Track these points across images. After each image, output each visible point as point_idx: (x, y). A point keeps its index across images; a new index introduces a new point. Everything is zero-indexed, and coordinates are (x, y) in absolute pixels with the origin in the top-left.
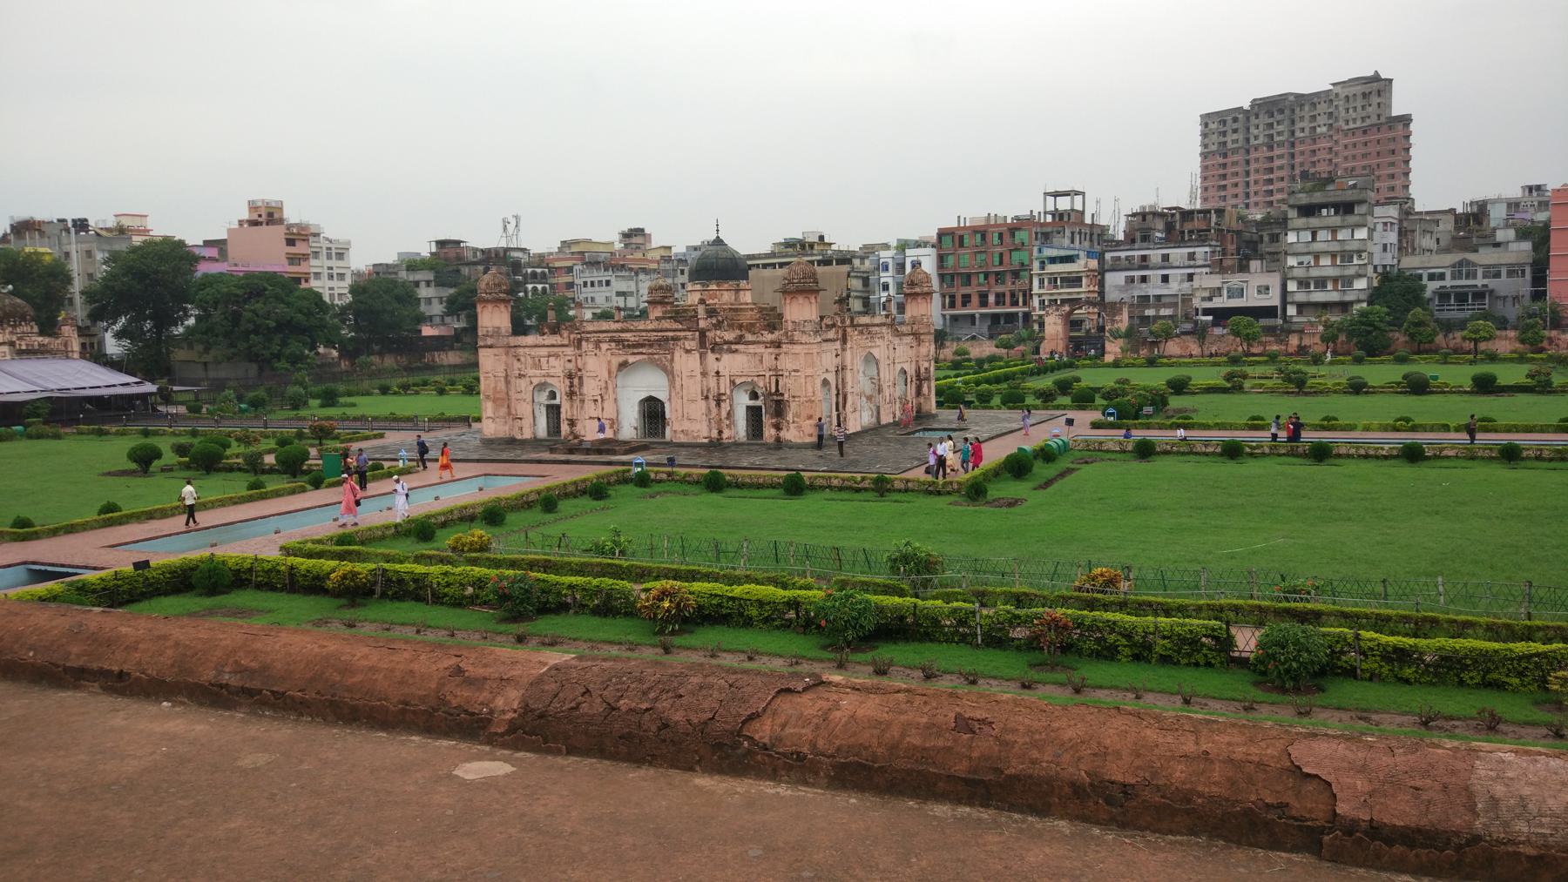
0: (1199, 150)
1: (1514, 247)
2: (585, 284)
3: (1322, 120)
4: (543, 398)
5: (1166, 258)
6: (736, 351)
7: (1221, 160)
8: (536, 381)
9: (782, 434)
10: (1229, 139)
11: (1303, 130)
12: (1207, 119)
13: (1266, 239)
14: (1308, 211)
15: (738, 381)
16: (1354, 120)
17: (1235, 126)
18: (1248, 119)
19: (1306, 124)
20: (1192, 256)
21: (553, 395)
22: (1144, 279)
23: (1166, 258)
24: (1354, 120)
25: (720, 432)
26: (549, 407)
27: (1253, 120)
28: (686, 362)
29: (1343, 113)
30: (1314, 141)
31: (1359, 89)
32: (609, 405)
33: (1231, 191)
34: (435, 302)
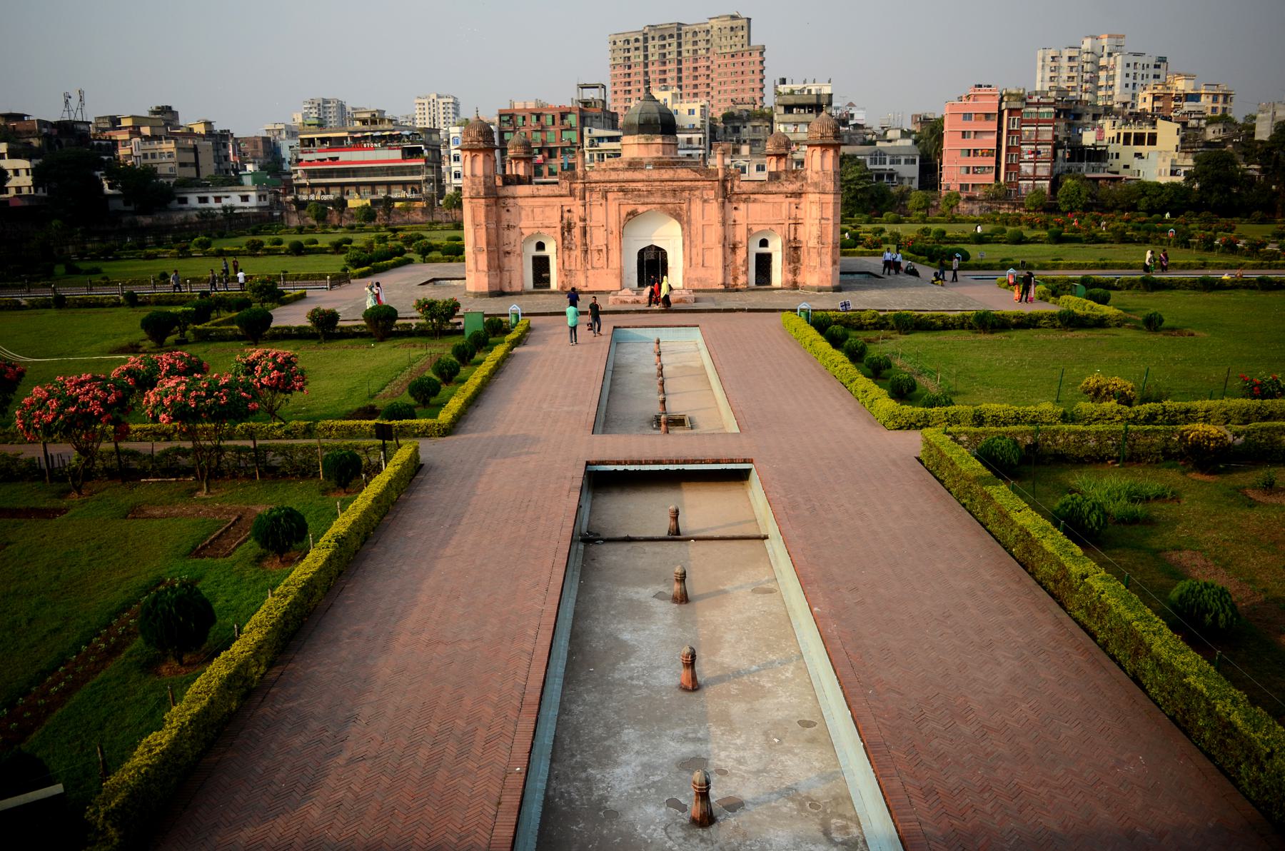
1: (901, 143)
2: (145, 156)
3: (702, 45)
4: (533, 251)
6: (755, 201)
7: (627, 71)
8: (527, 232)
9: (799, 279)
13: (730, 130)
14: (789, 109)
15: (755, 229)
17: (637, 45)
18: (646, 40)
19: (690, 47)
20: (689, 141)
21: (541, 246)
25: (735, 278)
26: (535, 258)
27: (650, 43)
28: (706, 212)
30: (696, 60)
31: (730, 23)
32: (614, 255)
33: (635, 95)
34: (23, 173)
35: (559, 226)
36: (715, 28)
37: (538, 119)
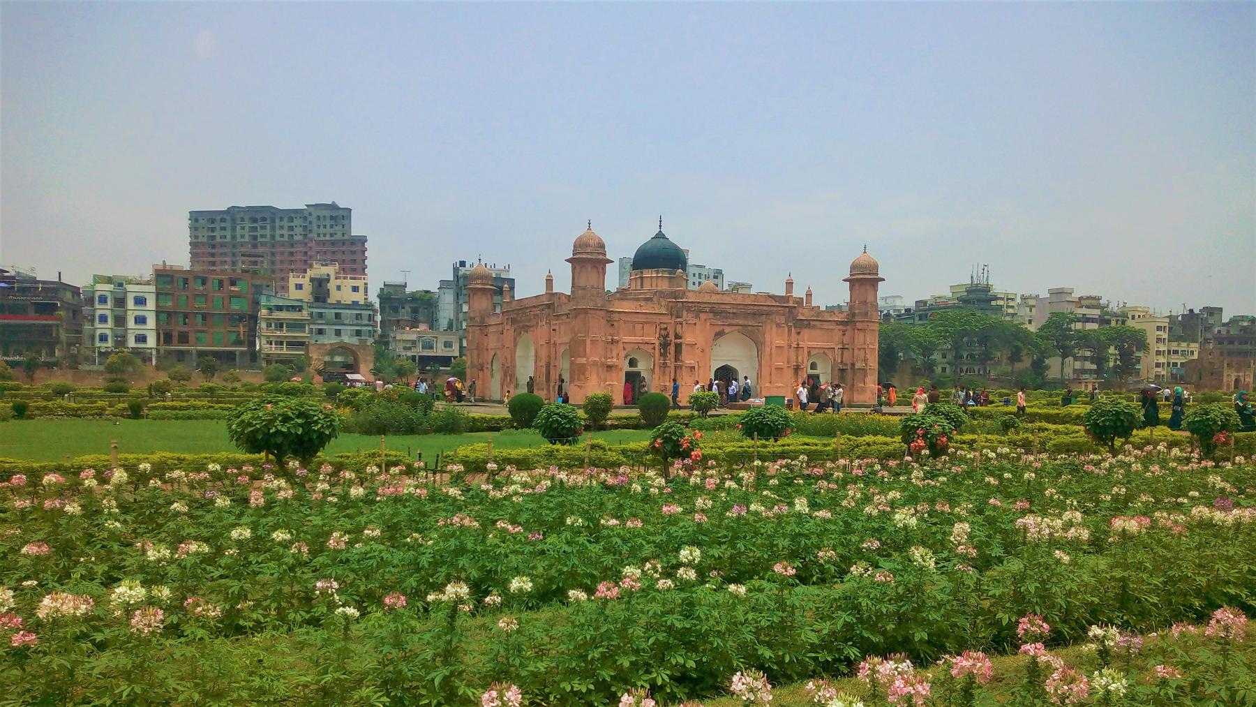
0: (189, 240)
5: (338, 316)
6: (814, 327)
7: (210, 250)
10: (217, 234)
11: (282, 236)
12: (196, 218)
16: (325, 235)
17: (223, 225)
19: (285, 232)
22: (320, 332)
23: (338, 316)
24: (325, 235)
26: (627, 373)
29: (315, 227)
31: (328, 213)
35: (657, 343)
36: (315, 215)
37: (204, 283)
